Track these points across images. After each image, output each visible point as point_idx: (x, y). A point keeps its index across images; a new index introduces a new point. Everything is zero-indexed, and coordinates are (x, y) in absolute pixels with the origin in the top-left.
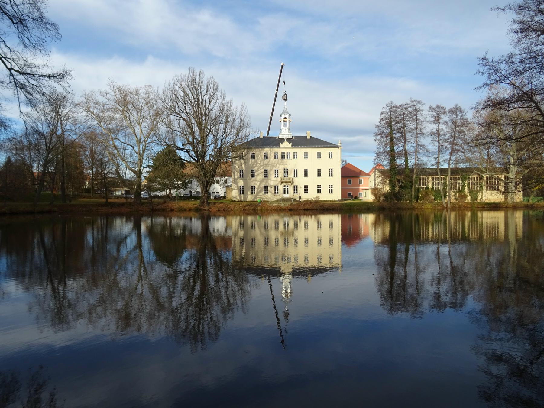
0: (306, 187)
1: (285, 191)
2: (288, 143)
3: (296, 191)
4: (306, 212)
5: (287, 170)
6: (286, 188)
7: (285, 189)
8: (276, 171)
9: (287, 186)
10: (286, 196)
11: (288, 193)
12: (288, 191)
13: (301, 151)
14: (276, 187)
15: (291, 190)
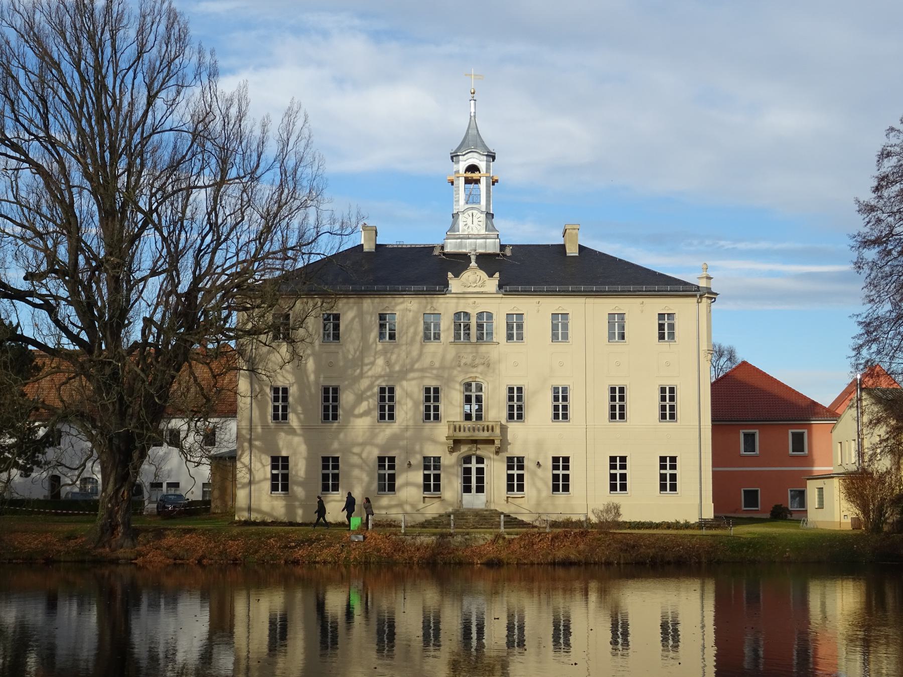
0: (561, 462)
1: (467, 480)
2: (483, 275)
3: (515, 484)
4: (560, 572)
5: (479, 388)
6: (474, 466)
7: (467, 471)
9: (480, 460)
10: (475, 501)
11: (480, 489)
12: (480, 480)
13: (537, 310)
15: (496, 472)
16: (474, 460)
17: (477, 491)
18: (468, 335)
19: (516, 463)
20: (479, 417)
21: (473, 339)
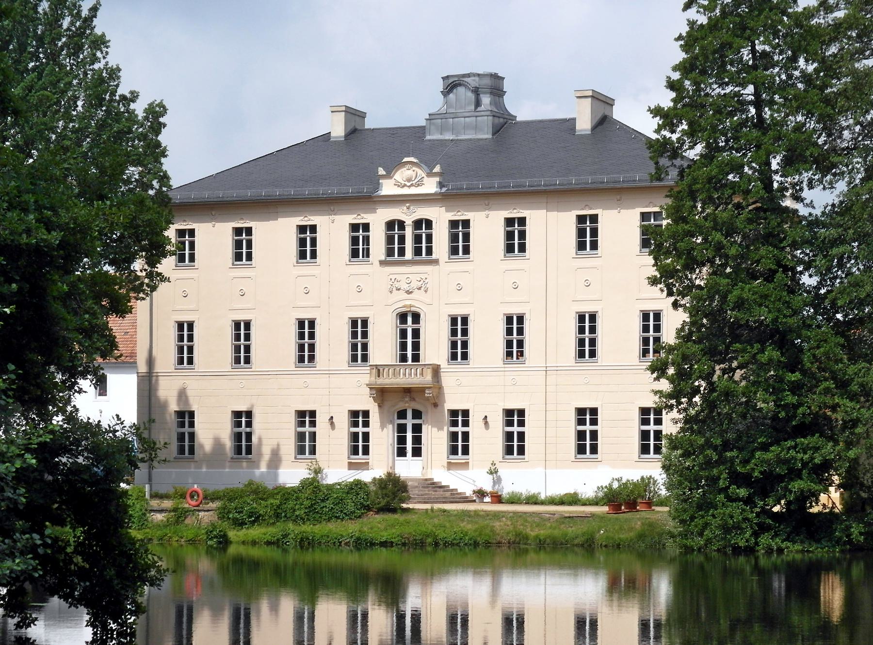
5: (416, 317)
6: (409, 422)
7: (402, 429)
8: (359, 328)
9: (417, 414)
11: (417, 452)
12: (417, 440)
14: (358, 417)
16: (409, 414)
17: (414, 455)
18: (402, 252)
19: (460, 417)
20: (416, 358)
21: (409, 254)
